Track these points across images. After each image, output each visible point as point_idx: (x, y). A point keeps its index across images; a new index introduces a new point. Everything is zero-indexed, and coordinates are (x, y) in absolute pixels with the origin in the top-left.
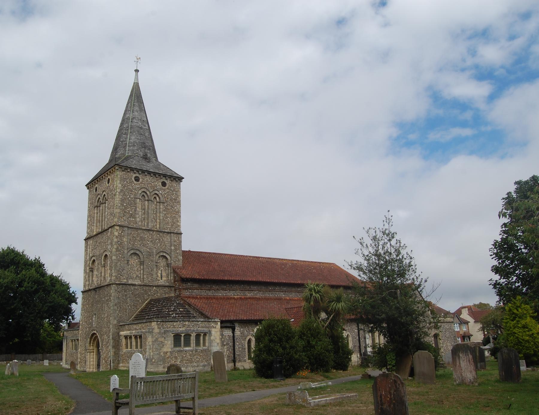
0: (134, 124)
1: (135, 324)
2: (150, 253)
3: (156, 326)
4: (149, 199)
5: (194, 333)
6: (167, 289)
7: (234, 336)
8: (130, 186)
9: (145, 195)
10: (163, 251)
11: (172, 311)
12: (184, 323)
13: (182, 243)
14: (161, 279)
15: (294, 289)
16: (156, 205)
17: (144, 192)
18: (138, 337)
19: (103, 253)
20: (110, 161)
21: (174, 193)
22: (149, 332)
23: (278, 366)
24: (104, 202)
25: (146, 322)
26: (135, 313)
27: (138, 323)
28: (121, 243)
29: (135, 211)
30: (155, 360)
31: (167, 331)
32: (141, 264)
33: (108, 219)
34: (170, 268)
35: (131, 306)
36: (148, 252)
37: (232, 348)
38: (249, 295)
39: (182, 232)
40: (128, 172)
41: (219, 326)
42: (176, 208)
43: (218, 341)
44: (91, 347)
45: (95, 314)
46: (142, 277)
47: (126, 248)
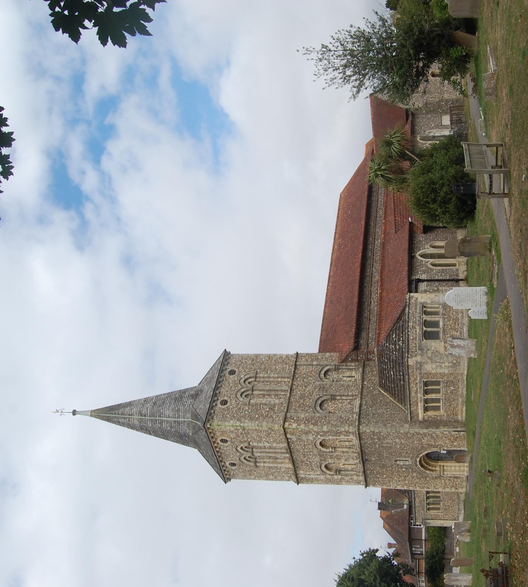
0: (149, 412)
1: (410, 394)
2: (320, 388)
3: (414, 359)
4: (251, 389)
5: (423, 317)
6: (367, 369)
7: (428, 281)
8: (233, 411)
9: (246, 393)
10: (318, 373)
11: (395, 346)
12: (411, 327)
13: (309, 353)
14: (354, 377)
15: (372, 230)
16: (259, 382)
17: (241, 395)
18: (426, 388)
19: (318, 449)
20: (196, 444)
21: (244, 361)
22: (420, 369)
23: (462, 188)
24: (251, 450)
25: (409, 375)
26: (396, 404)
28: (306, 420)
29: (266, 405)
30: (454, 359)
31: (419, 347)
32: (334, 398)
33: (274, 442)
34: (340, 367)
35: (388, 409)
36: (319, 390)
37: (441, 283)
38: (377, 277)
39: (296, 352)
40: (214, 412)
41: (415, 294)
42: (264, 359)
43: (433, 295)
44: (437, 469)
45: (396, 461)
46: (351, 398)
47: (313, 414)
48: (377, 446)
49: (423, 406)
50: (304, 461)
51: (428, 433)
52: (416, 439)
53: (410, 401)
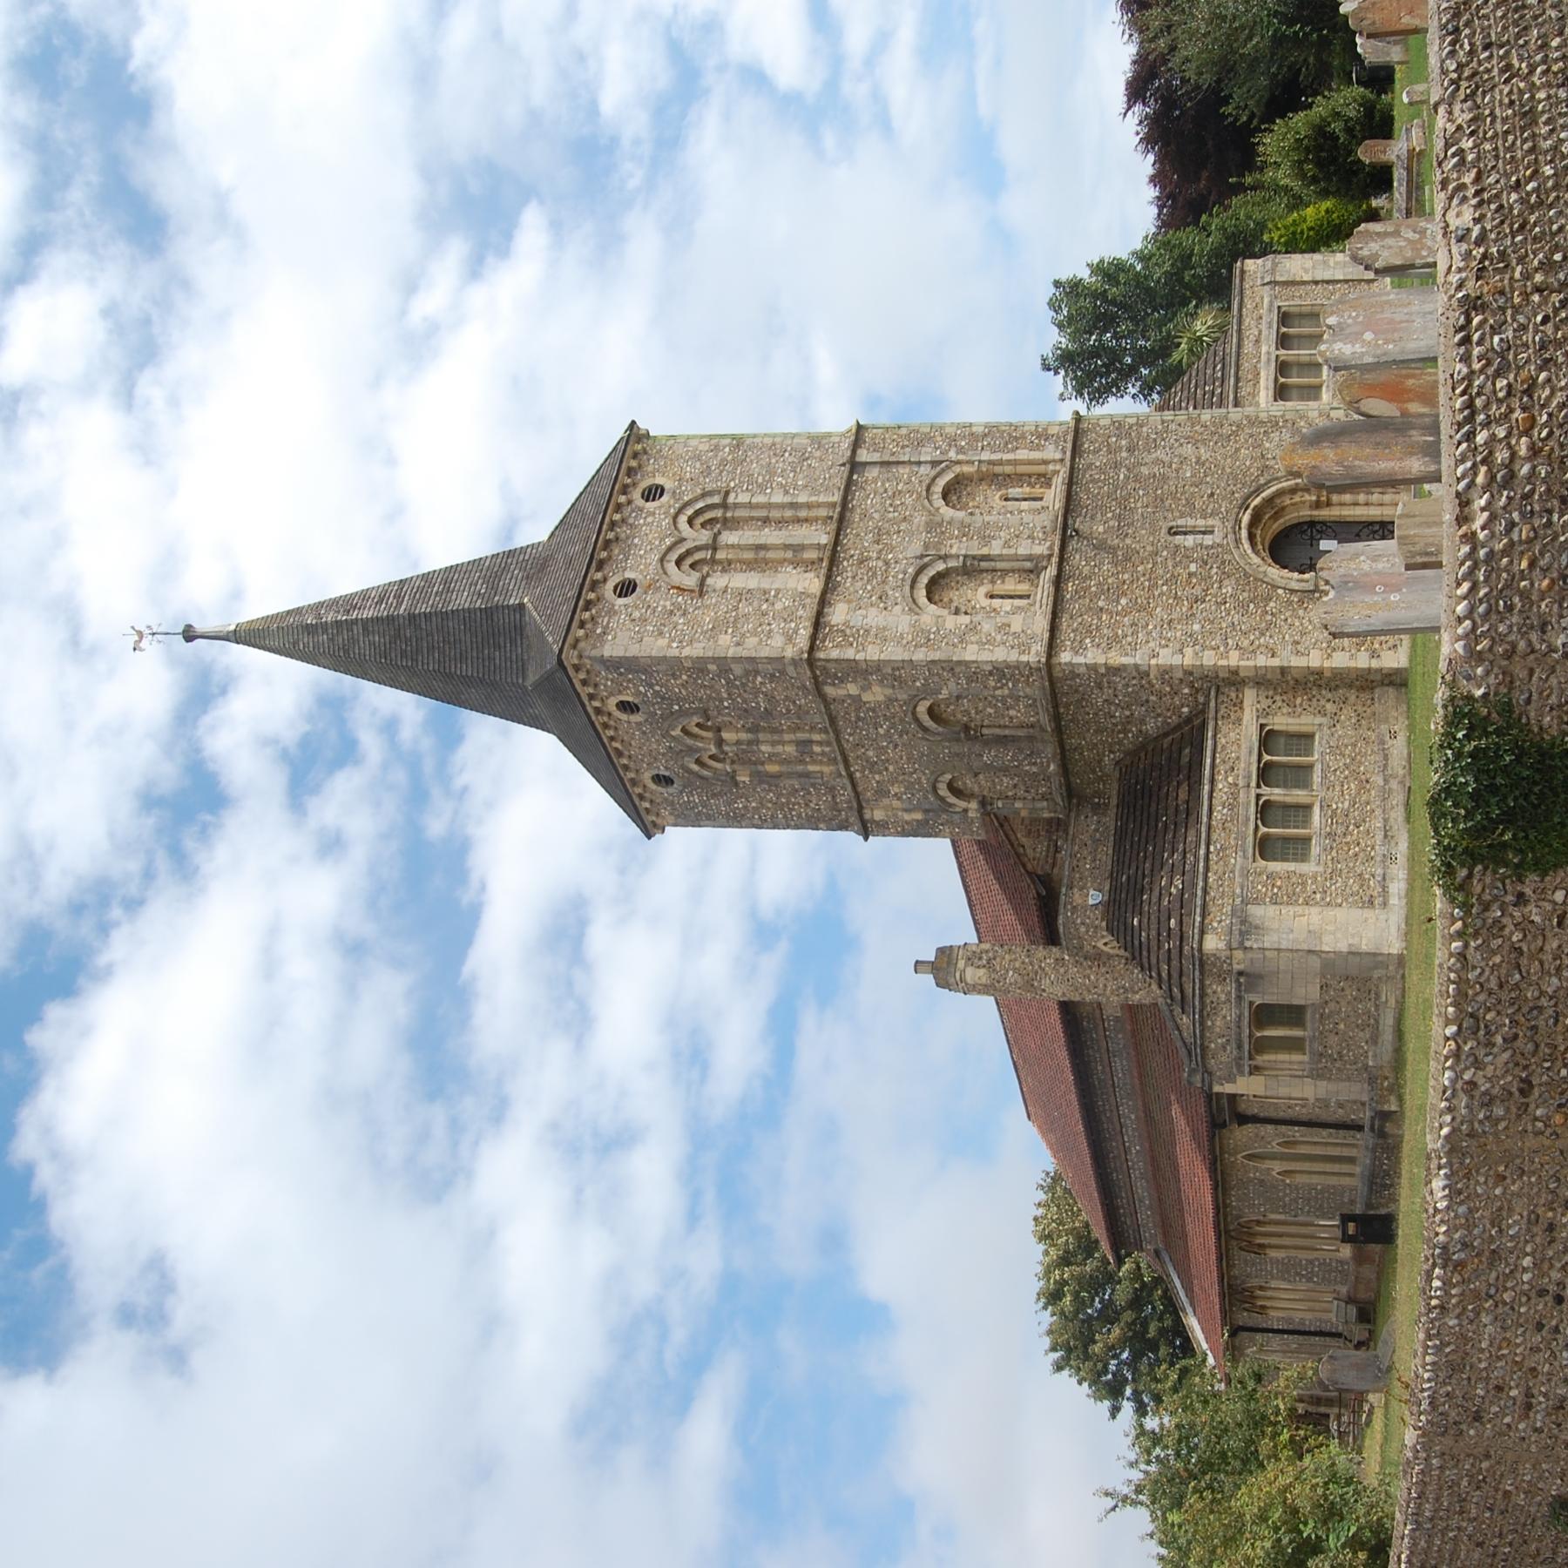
1: (1239, 346)
18: (1284, 330)
27: (1239, 331)
45: (1173, 532)
48: (1122, 477)
50: (868, 559)
51: (1282, 416)
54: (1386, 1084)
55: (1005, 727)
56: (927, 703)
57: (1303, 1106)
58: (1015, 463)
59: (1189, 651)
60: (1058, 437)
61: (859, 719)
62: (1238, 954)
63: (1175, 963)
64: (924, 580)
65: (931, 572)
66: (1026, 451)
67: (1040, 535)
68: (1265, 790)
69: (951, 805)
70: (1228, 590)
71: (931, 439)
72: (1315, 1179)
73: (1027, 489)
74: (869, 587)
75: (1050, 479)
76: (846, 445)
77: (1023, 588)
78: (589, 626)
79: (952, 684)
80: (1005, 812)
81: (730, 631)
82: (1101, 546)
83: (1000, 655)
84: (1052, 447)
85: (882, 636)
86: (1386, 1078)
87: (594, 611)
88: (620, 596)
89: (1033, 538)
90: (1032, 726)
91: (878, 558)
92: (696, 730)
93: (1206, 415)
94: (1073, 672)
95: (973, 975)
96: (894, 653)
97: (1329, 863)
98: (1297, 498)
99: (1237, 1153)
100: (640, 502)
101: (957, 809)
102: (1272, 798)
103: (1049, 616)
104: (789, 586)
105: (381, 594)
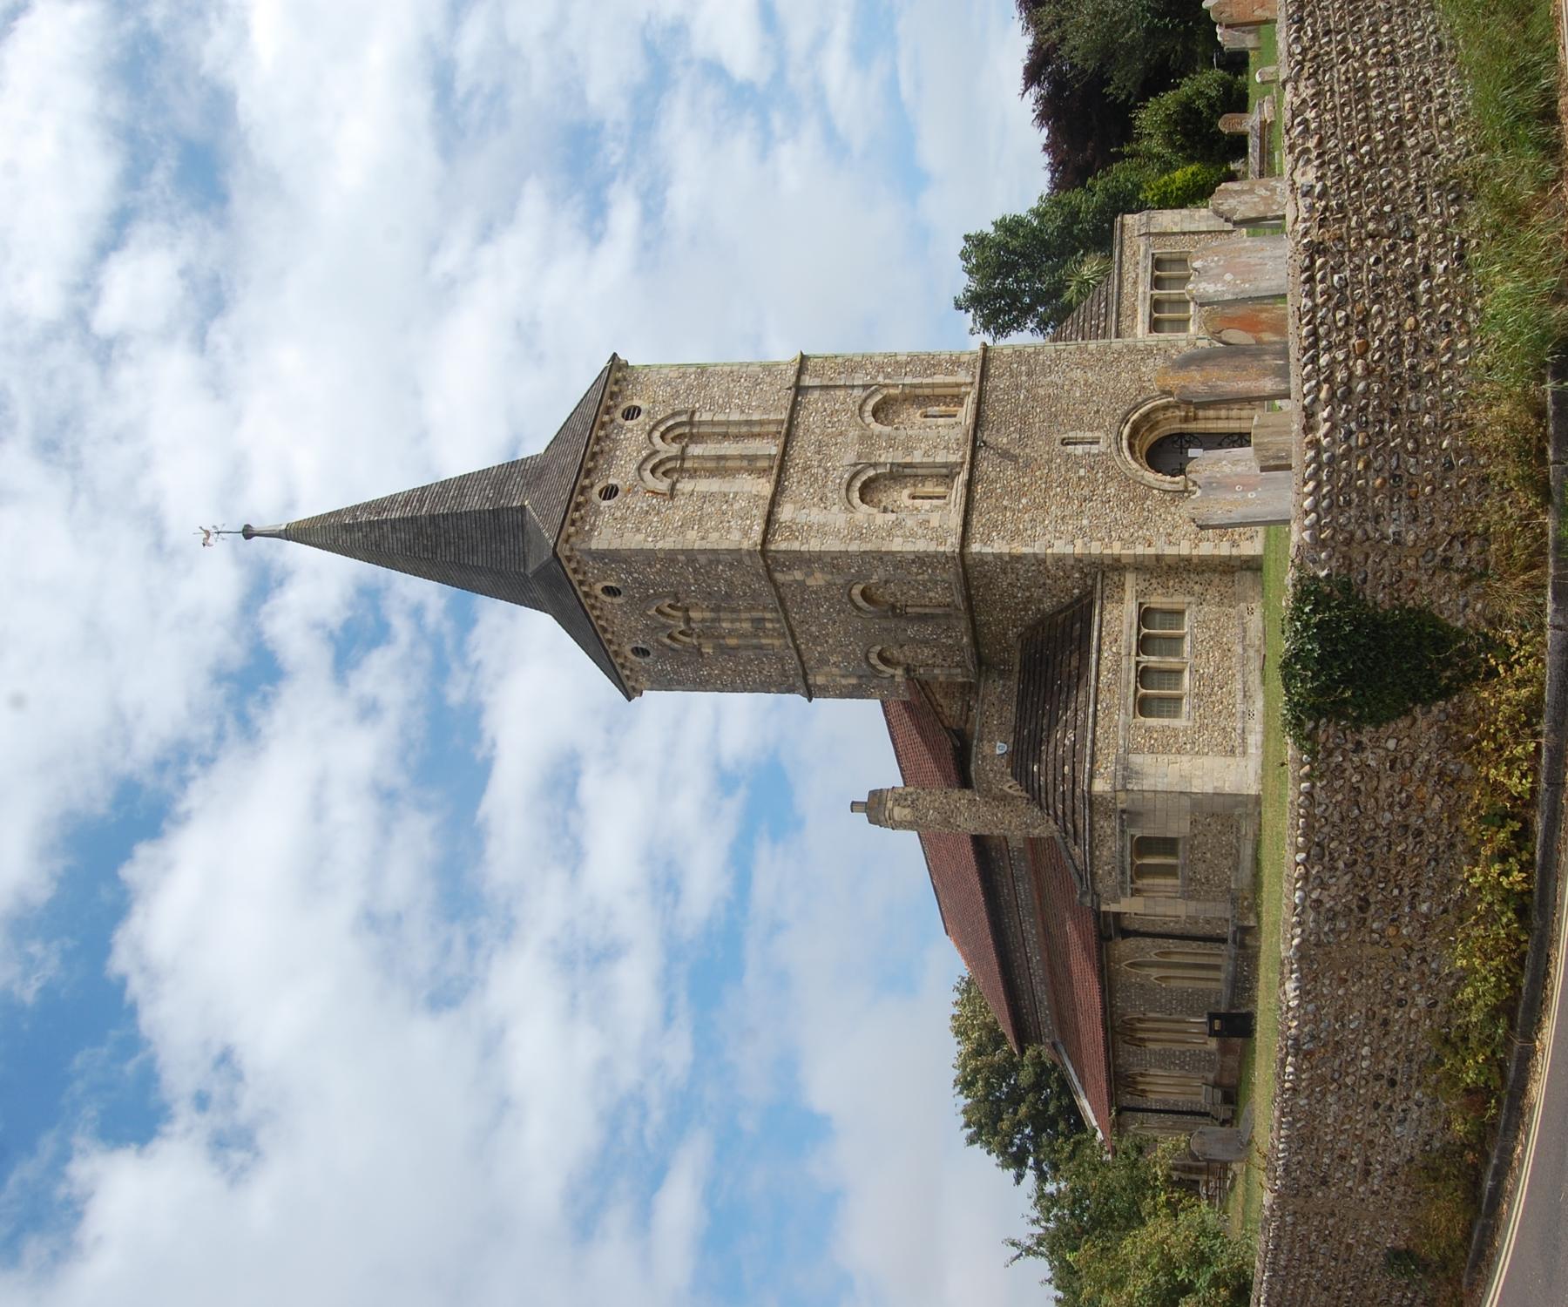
1: (1120, 287)
27: (1120, 274)
45: (1065, 442)
48: (1022, 397)
49: (1148, 313)
51: (1156, 346)
52: (1126, 366)
53: (1119, 304)
54: (1246, 903)
55: (926, 606)
56: (861, 587)
57: (1176, 923)
58: (933, 386)
59: (1079, 542)
60: (969, 364)
61: (803, 600)
62: (1122, 796)
63: (1068, 803)
64: (858, 484)
65: (864, 478)
66: (942, 376)
67: (954, 446)
68: (1144, 658)
69: (881, 672)
70: (1111, 491)
71: (863, 367)
72: (1187, 984)
73: (943, 408)
74: (812, 491)
75: (962, 399)
76: (792, 372)
77: (940, 490)
78: (578, 524)
79: (881, 571)
80: (925, 678)
81: (696, 527)
82: (1005, 455)
83: (921, 546)
84: (963, 373)
85: (822, 531)
86: (1246, 899)
87: (583, 512)
88: (604, 499)
89: (948, 449)
90: (948, 606)
91: (819, 466)
92: (668, 610)
93: (1092, 345)
94: (982, 559)
95: (898, 813)
96: (833, 545)
97: (1198, 720)
98: (1169, 414)
99: (1119, 962)
100: (620, 421)
101: (886, 675)
102: (1150, 665)
103: (962, 514)
104: (744, 490)
105: (408, 498)
